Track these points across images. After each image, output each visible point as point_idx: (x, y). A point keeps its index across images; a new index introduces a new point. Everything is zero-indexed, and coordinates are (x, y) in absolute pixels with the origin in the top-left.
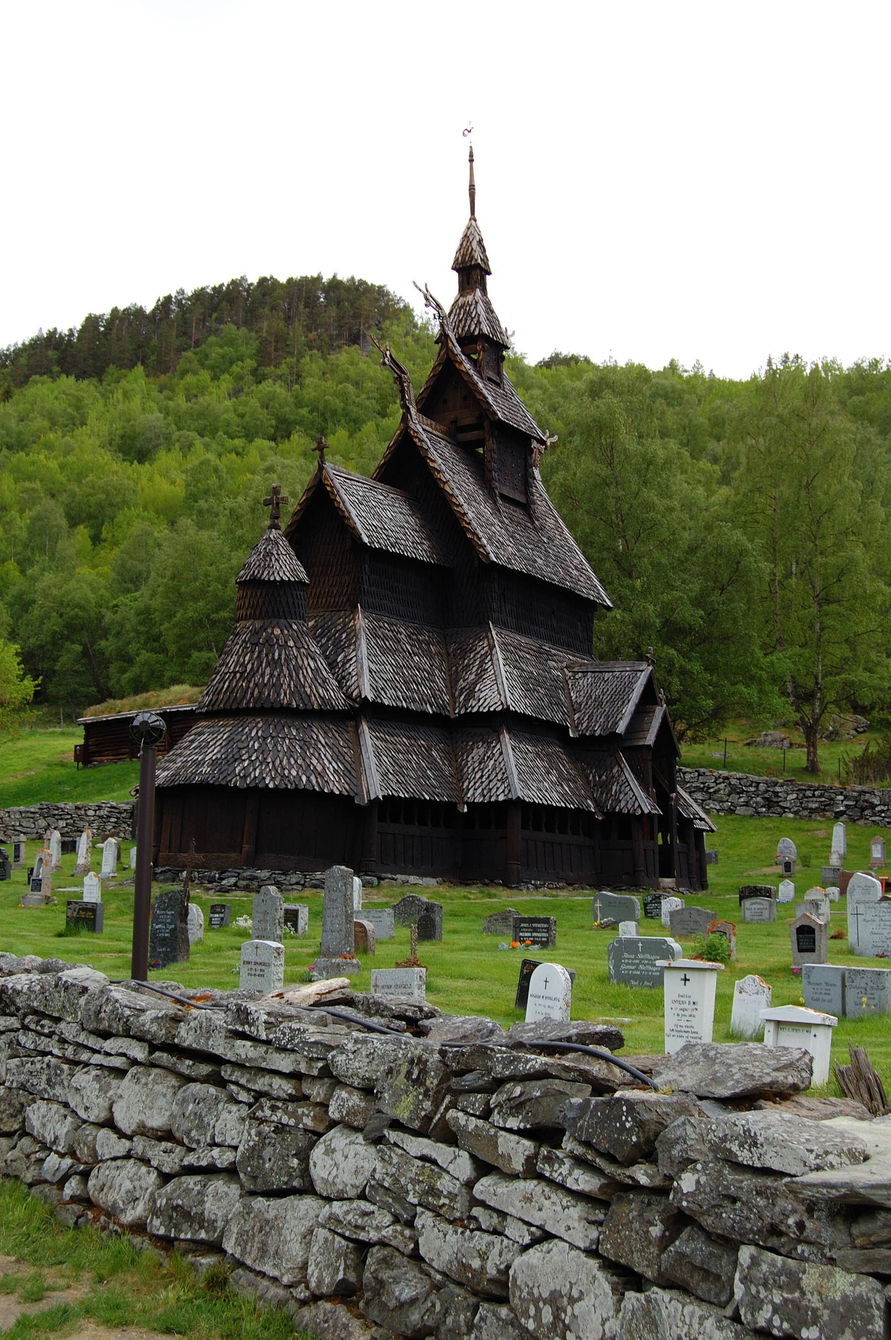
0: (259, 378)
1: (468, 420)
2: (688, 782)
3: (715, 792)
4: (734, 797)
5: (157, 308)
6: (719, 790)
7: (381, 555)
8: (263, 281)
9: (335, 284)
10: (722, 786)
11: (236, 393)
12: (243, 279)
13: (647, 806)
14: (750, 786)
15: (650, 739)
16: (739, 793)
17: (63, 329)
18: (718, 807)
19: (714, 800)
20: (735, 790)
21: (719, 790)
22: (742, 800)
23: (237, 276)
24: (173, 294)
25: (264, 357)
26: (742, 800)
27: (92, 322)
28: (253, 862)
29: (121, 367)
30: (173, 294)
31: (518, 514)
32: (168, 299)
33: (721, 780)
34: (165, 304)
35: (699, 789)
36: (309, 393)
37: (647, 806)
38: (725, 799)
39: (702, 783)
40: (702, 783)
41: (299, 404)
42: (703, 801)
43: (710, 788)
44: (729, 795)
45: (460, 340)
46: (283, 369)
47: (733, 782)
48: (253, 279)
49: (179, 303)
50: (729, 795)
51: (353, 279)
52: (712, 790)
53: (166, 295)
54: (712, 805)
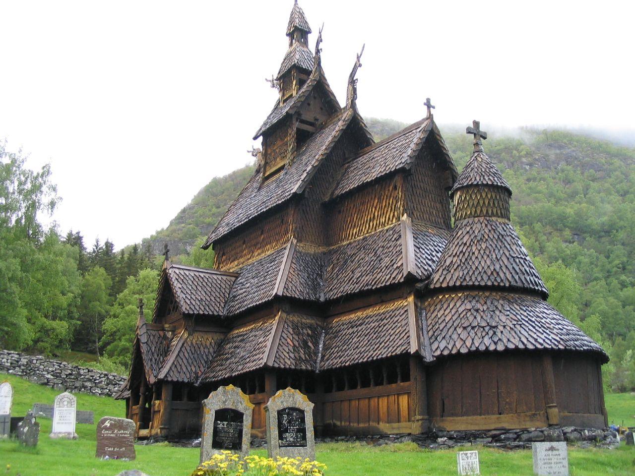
2: (82, 375)
3: (99, 383)
4: (111, 387)
6: (102, 381)
10: (103, 379)
14: (121, 381)
16: (114, 385)
18: (100, 392)
19: (97, 387)
21: (102, 381)
22: (116, 389)
26: (116, 389)
33: (103, 376)
35: (89, 380)
38: (105, 387)
39: (91, 376)
40: (91, 376)
42: (91, 387)
43: (95, 380)
44: (108, 384)
47: (111, 377)
50: (108, 384)
52: (97, 381)
54: (96, 391)
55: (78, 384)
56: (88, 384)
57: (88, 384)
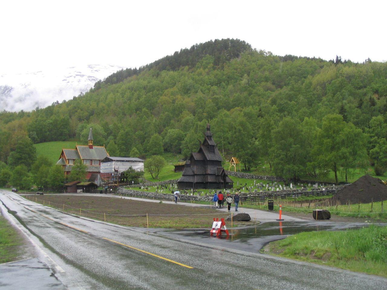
0: (214, 69)
1: (207, 144)
5: (191, 48)
7: (197, 160)
8: (216, 40)
9: (232, 41)
11: (208, 74)
12: (211, 40)
13: (222, 181)
15: (223, 175)
17: (170, 55)
20: (249, 176)
23: (209, 40)
24: (195, 45)
25: (216, 63)
27: (176, 53)
28: (186, 187)
29: (183, 66)
30: (195, 45)
31: (213, 153)
32: (194, 46)
34: (193, 47)
36: (225, 73)
37: (222, 181)
41: (224, 75)
45: (207, 136)
46: (220, 66)
48: (213, 41)
49: (196, 46)
51: (237, 39)
53: (193, 45)
55: (243, 177)
56: (245, 177)
57: (245, 177)
